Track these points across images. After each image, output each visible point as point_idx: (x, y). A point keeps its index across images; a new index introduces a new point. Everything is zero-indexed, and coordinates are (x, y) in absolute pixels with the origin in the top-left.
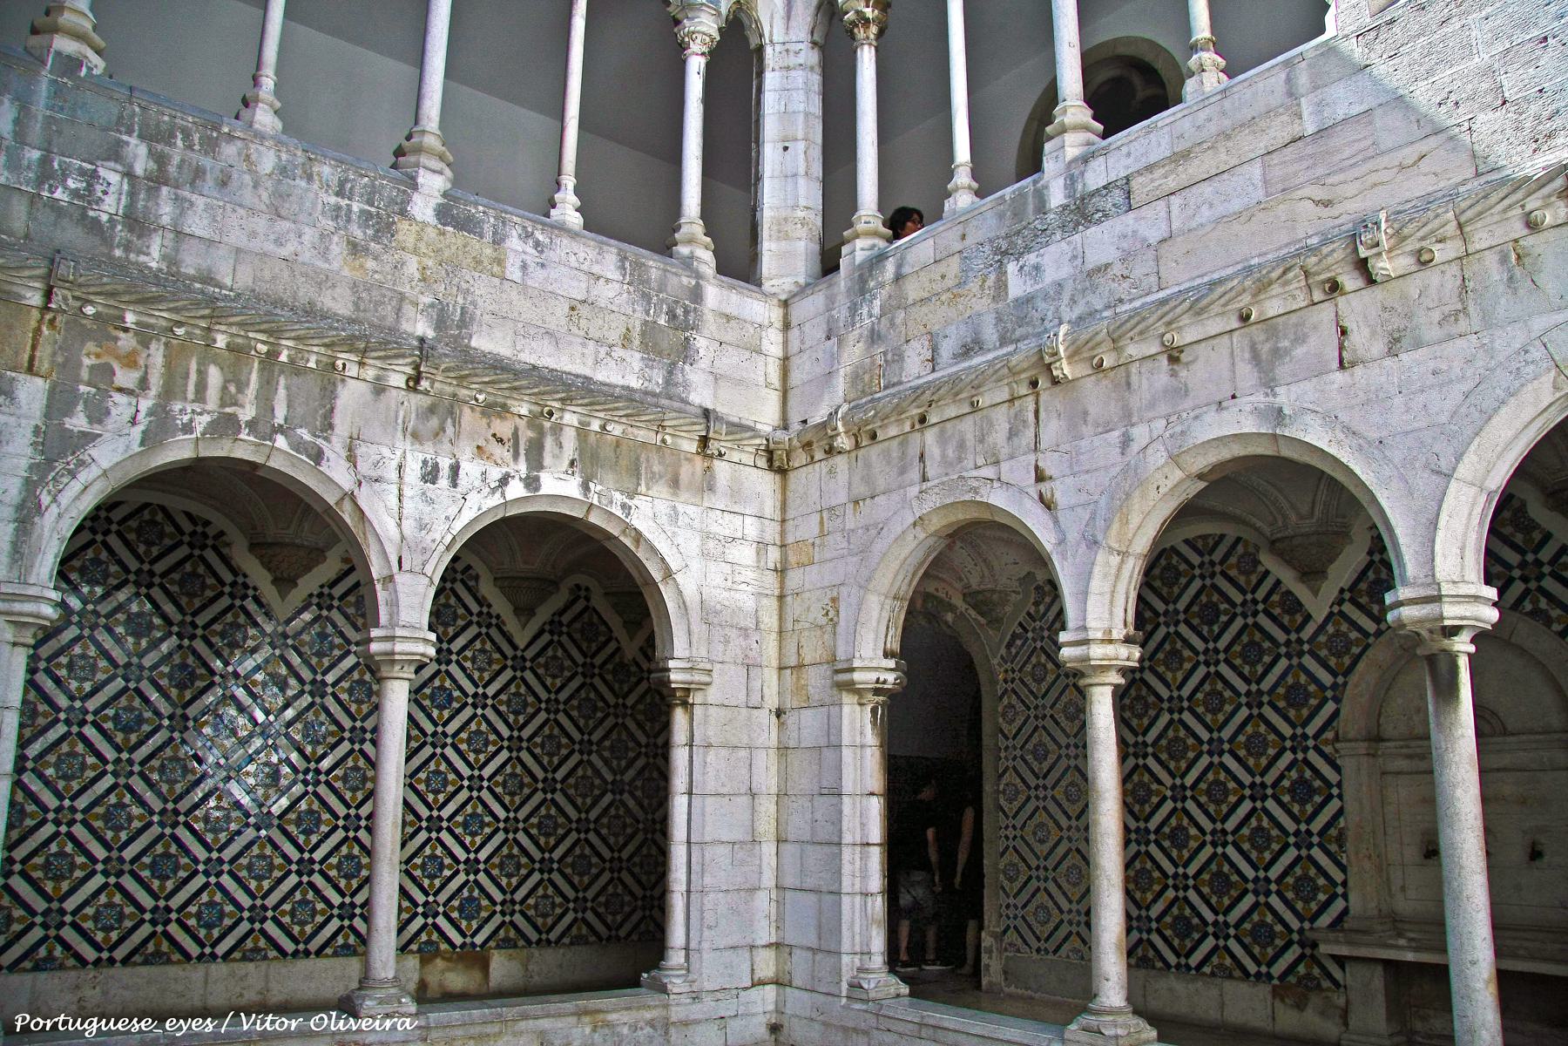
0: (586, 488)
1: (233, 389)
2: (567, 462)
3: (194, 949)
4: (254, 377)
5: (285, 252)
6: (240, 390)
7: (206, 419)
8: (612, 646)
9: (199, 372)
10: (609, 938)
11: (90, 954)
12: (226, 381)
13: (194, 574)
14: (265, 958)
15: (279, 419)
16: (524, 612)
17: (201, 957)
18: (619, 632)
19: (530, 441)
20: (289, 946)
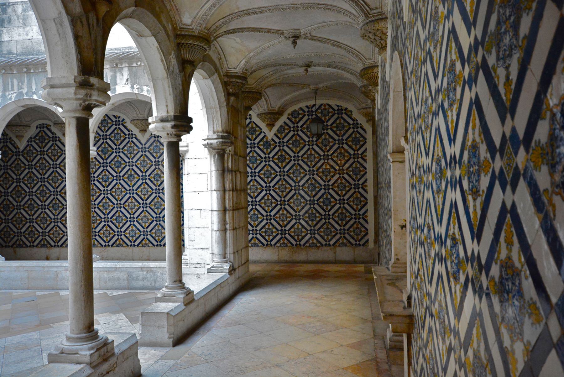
0: (132, 87)
1: (20, 84)
2: (125, 80)
3: (129, 243)
4: (26, 79)
5: (29, 37)
6: (22, 84)
7: (15, 95)
8: (262, 135)
9: (11, 82)
10: (267, 245)
11: (103, 244)
12: (19, 82)
13: (118, 133)
14: (149, 246)
15: (34, 90)
16: (271, 125)
17: (131, 245)
18: (265, 128)
19: (112, 76)
20: (155, 243)
